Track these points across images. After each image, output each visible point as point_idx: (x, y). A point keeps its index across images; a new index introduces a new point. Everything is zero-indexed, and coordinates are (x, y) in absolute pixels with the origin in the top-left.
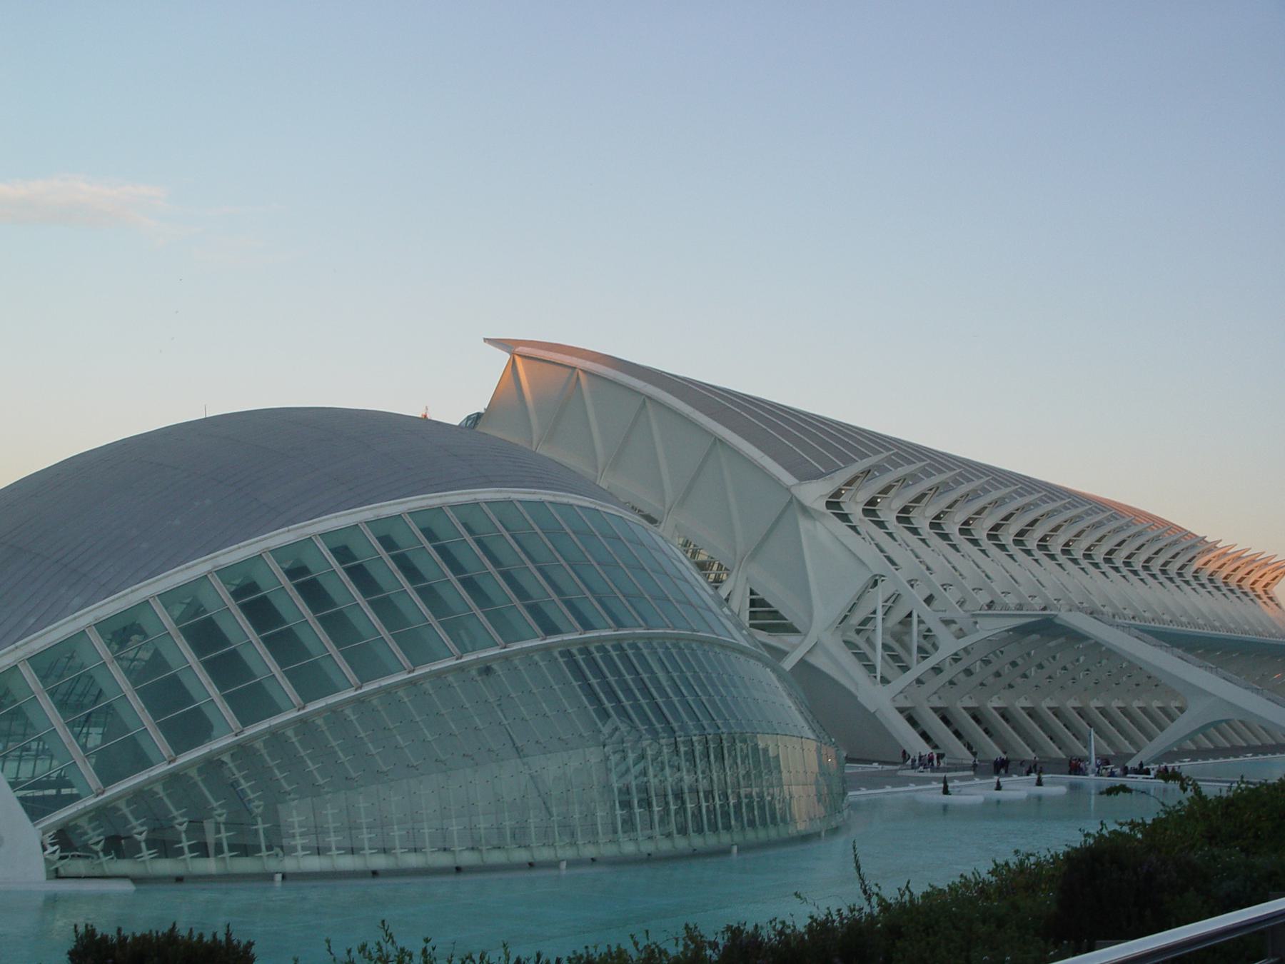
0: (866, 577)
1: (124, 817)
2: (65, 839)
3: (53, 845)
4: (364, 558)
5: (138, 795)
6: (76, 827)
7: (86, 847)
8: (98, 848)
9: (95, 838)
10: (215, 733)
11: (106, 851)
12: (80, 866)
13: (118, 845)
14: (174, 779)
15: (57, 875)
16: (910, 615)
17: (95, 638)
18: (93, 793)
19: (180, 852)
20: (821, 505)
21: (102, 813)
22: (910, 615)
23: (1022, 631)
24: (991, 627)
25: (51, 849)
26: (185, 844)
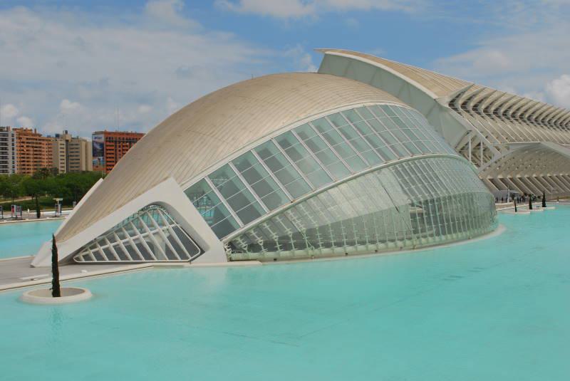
0: (463, 132)
1: (254, 237)
2: (232, 245)
3: (228, 248)
4: (328, 131)
5: (258, 227)
6: (235, 241)
7: (241, 249)
8: (246, 249)
9: (244, 244)
10: (282, 202)
11: (249, 251)
12: (239, 256)
13: (253, 247)
14: (270, 220)
15: (231, 260)
16: (479, 144)
17: (232, 166)
18: (242, 227)
19: (276, 249)
20: (447, 106)
21: (245, 235)
22: (479, 144)
23: (523, 150)
24: (513, 149)
25: (228, 250)
26: (278, 246)
